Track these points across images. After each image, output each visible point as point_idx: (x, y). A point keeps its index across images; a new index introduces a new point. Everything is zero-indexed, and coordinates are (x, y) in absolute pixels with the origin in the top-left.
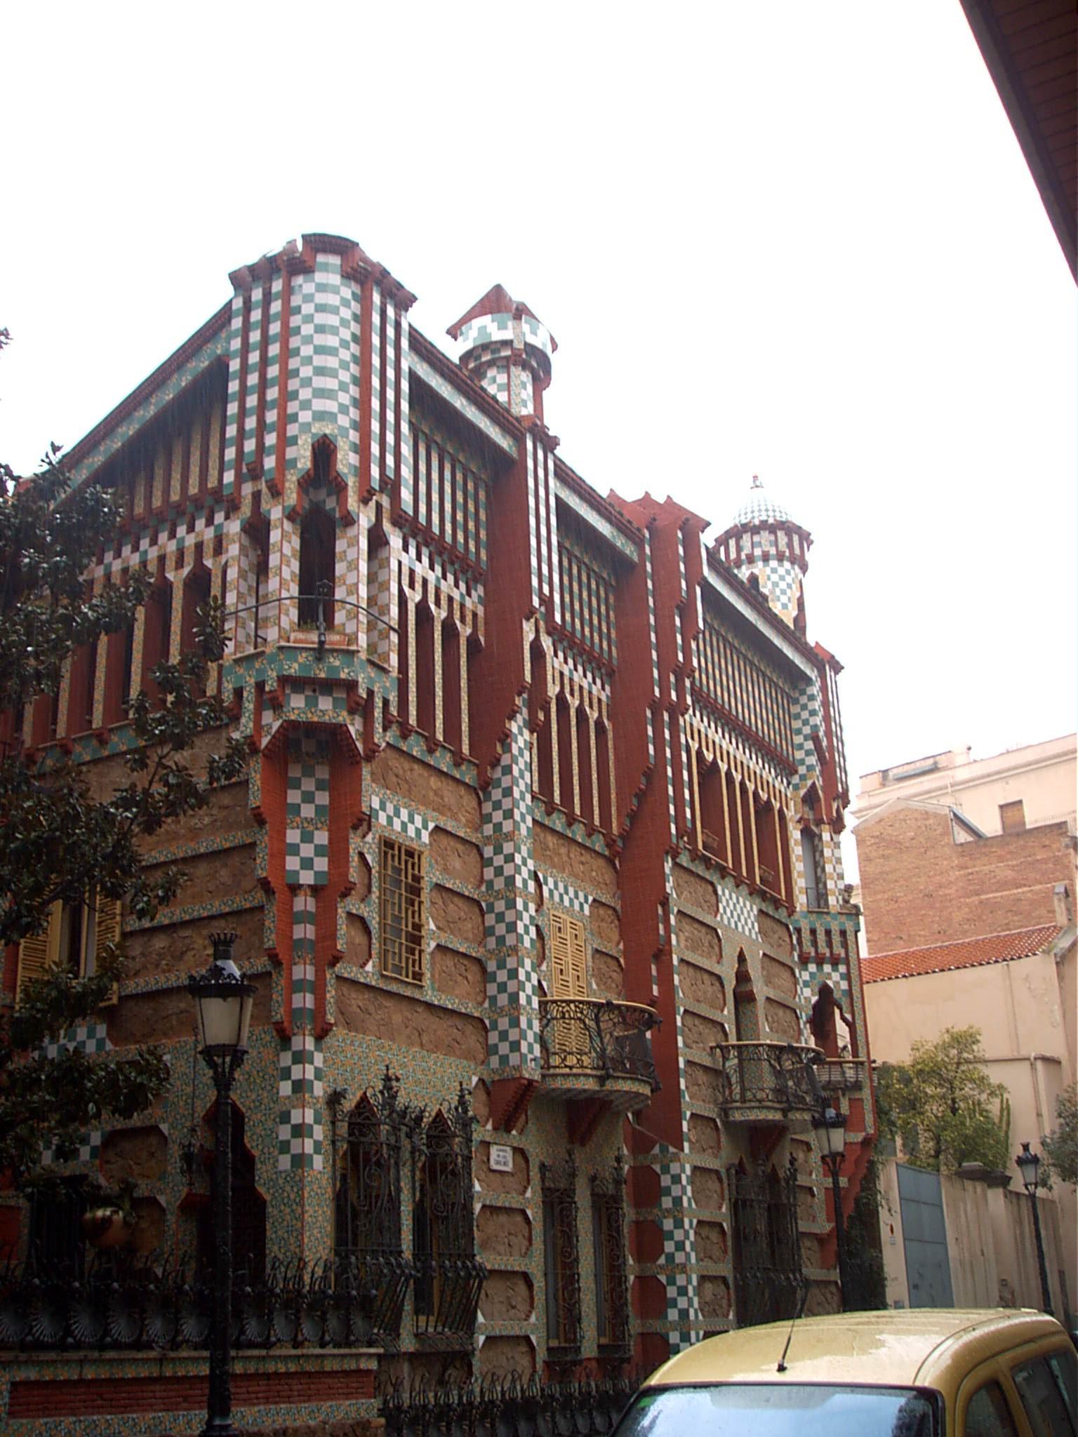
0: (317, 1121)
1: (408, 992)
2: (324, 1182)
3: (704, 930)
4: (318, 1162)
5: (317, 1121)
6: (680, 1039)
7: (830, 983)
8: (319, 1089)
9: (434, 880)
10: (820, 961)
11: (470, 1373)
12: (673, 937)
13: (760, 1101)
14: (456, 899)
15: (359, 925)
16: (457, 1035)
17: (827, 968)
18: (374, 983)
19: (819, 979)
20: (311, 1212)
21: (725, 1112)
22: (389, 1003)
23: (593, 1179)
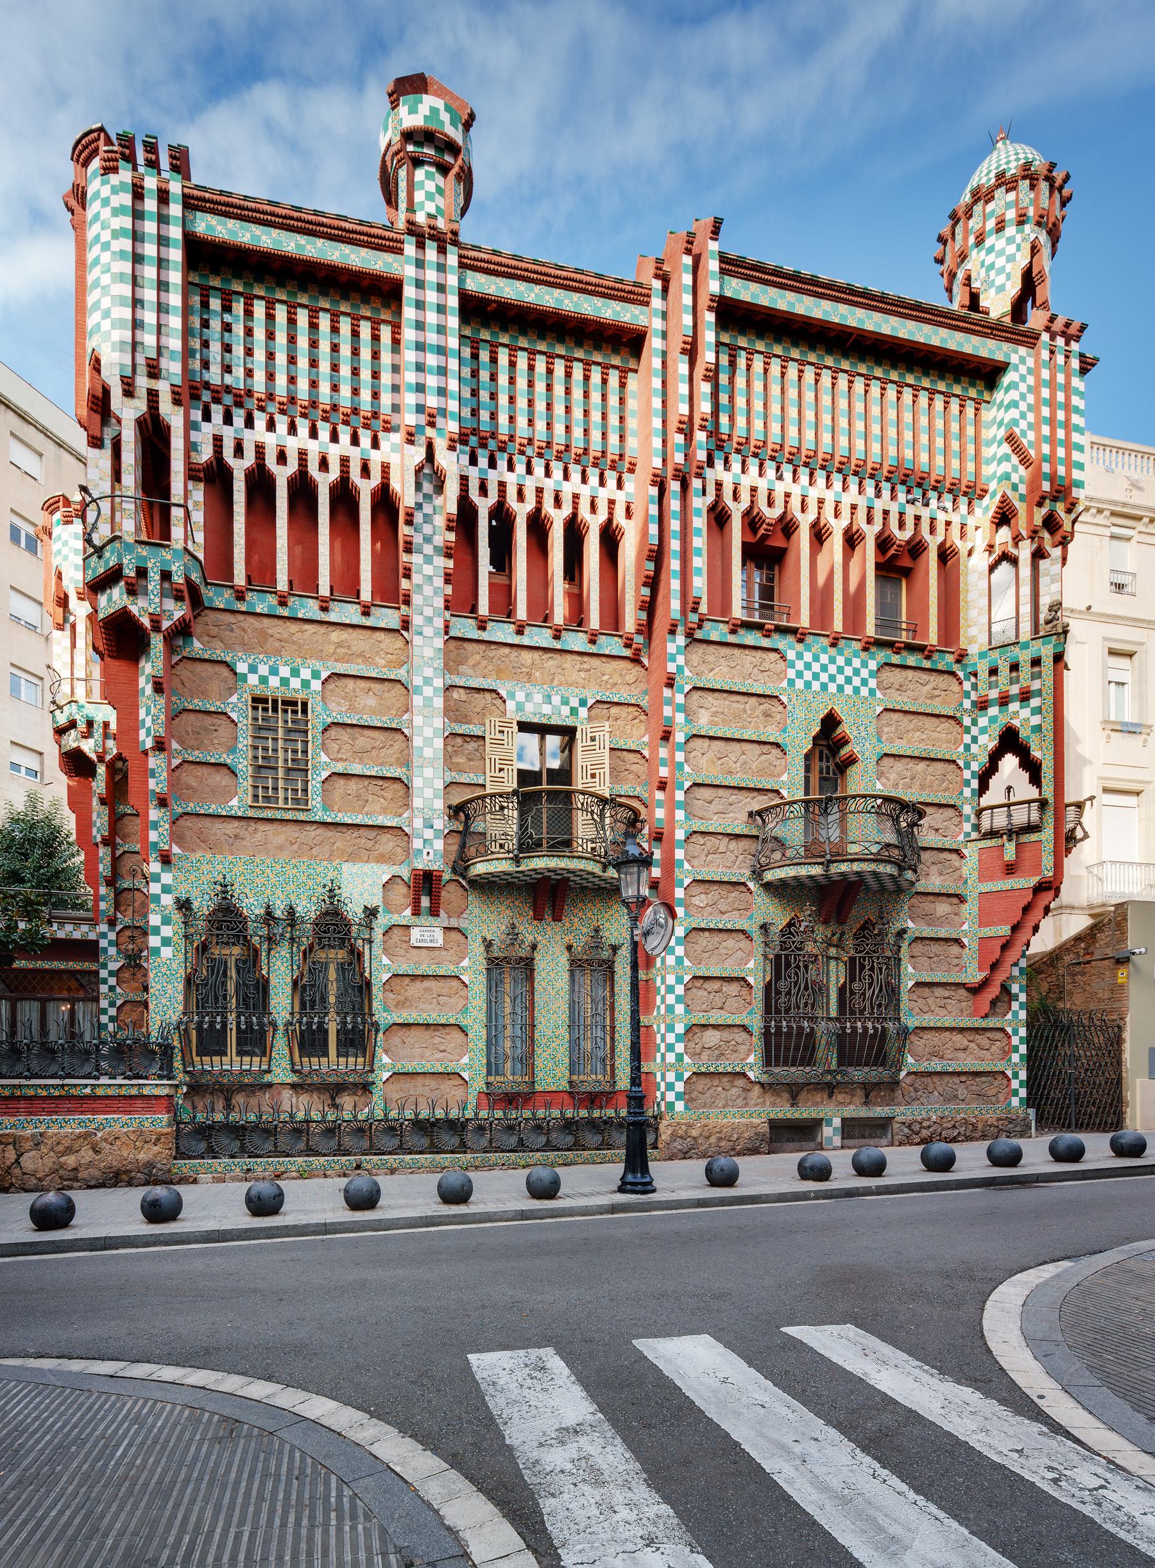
0: (166, 921)
1: (290, 815)
2: (174, 966)
3: (753, 700)
4: (167, 952)
5: (166, 921)
6: (680, 815)
7: (1016, 723)
8: (167, 900)
9: (329, 720)
10: (1004, 701)
12: (680, 718)
13: (791, 859)
14: (367, 732)
15: (225, 771)
17: (1014, 706)
19: (1003, 721)
21: (757, 874)
22: (262, 827)
23: (569, 948)
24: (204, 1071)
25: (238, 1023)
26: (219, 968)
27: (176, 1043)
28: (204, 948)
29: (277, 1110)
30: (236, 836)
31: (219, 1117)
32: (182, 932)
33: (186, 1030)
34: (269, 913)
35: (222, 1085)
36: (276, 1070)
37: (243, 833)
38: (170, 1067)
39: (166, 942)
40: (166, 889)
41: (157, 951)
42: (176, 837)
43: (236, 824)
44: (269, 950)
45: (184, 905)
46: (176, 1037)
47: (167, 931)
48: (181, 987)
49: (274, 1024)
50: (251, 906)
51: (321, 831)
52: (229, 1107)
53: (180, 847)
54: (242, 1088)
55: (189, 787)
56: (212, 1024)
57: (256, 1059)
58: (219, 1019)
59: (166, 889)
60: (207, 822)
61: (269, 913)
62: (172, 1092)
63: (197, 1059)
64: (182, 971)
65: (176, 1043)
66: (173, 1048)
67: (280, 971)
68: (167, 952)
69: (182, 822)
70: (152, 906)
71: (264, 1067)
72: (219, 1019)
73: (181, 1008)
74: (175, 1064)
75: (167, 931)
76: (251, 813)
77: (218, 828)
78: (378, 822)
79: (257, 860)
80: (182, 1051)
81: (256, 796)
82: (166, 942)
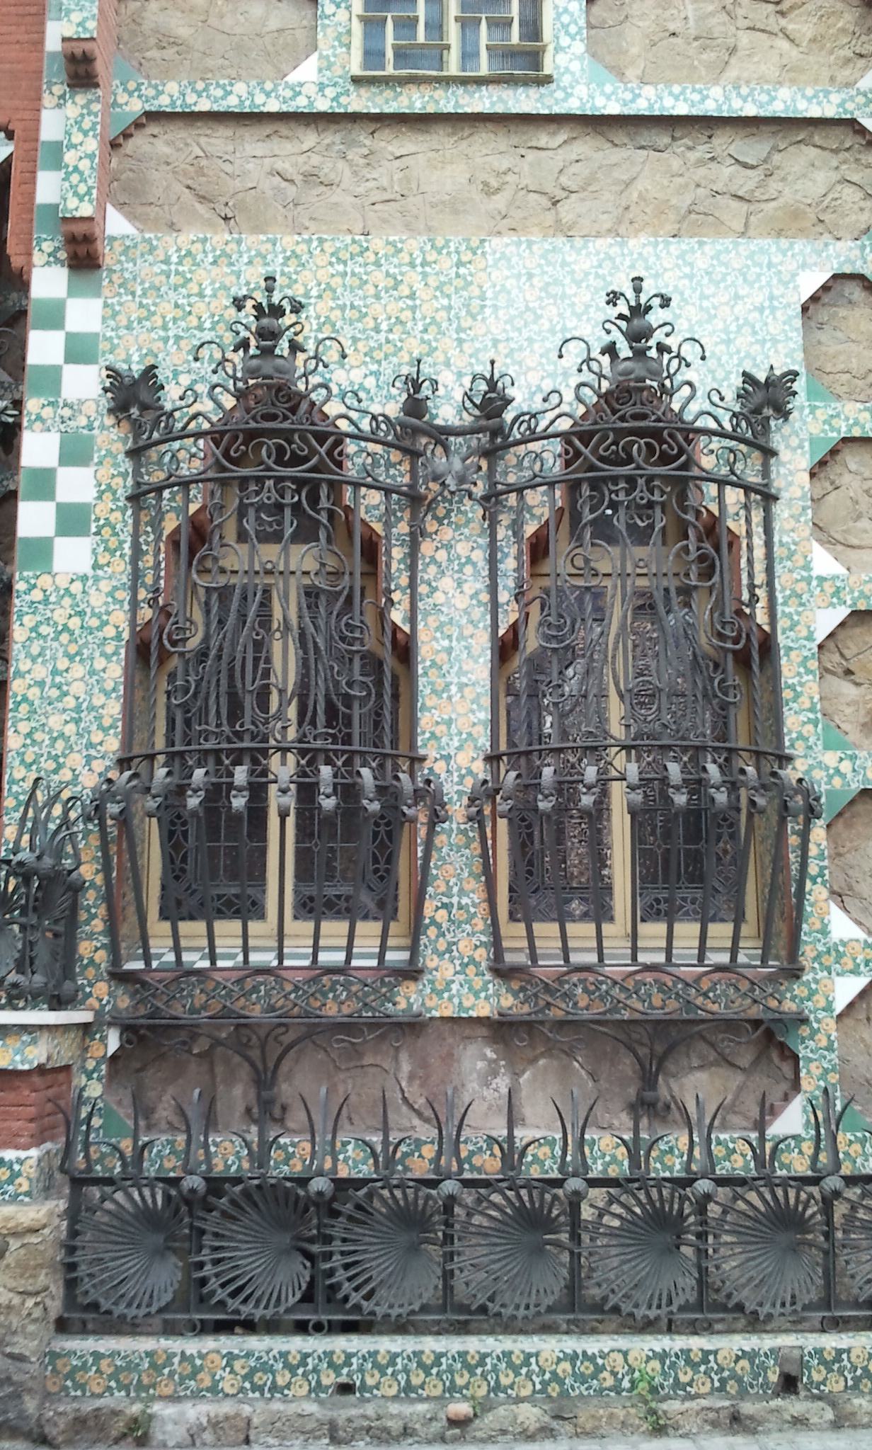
0: (75, 452)
2: (97, 600)
4: (73, 555)
5: (75, 452)
8: (84, 385)
11: (796, 1086)
16: (747, 182)
18: (322, 106)
20: (40, 672)
22: (392, 144)
24: (184, 973)
25: (307, 792)
26: (243, 607)
27: (88, 872)
28: (197, 536)
29: (448, 1121)
30: (311, 177)
31: (228, 1153)
32: (124, 487)
33: (124, 820)
34: (415, 407)
35: (243, 1026)
36: (440, 968)
37: (331, 167)
38: (66, 960)
39: (73, 520)
40: (79, 350)
41: (42, 549)
42: (120, 188)
43: (309, 138)
44: (416, 537)
45: (133, 396)
46: (89, 847)
47: (77, 485)
48: (116, 671)
49: (430, 796)
50: (353, 384)
51: (586, 147)
52: (267, 1111)
53: (132, 217)
54: (319, 1032)
55: (166, 41)
56: (218, 792)
57: (368, 931)
58: (241, 775)
59: (79, 350)
60: (218, 140)
61: (415, 407)
62: (64, 1052)
63: (159, 930)
64: (120, 618)
65: (88, 872)
66: (77, 889)
67: (454, 608)
68: (73, 555)
69: (139, 143)
70: (32, 405)
71: (395, 957)
72: (241, 775)
73: (113, 744)
74: (85, 948)
75: (77, 485)
76: (359, 101)
77: (254, 156)
78: (777, 109)
79: (377, 243)
80: (109, 898)
81: (372, 55)
82: (73, 520)
